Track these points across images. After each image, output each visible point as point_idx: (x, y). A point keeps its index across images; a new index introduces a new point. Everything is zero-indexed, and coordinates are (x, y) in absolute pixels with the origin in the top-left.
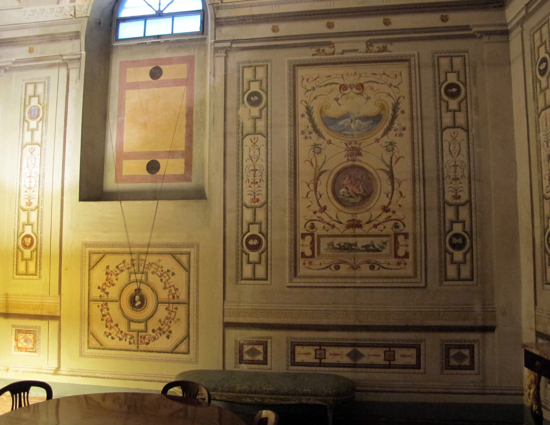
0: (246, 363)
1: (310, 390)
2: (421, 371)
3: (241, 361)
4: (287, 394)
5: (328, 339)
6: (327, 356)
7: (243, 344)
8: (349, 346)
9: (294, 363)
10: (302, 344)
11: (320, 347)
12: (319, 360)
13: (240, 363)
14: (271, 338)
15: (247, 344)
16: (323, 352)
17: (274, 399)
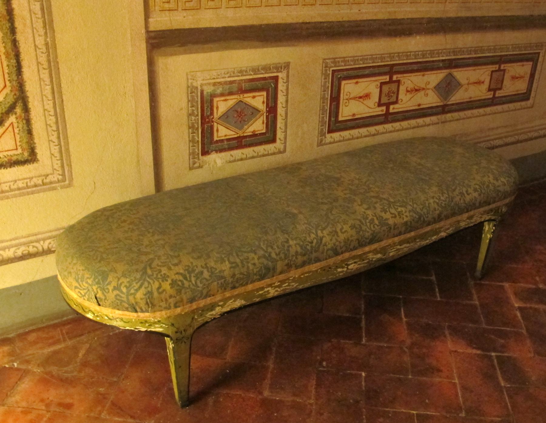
0: (221, 150)
1: (476, 194)
2: (529, 103)
3: (208, 144)
4: (439, 219)
5: (407, 54)
6: (400, 97)
7: (213, 96)
8: (439, 68)
9: (335, 124)
10: (357, 74)
11: (391, 78)
12: (384, 108)
13: (205, 153)
14: (287, 66)
15: (222, 95)
16: (394, 87)
17: (407, 241)
